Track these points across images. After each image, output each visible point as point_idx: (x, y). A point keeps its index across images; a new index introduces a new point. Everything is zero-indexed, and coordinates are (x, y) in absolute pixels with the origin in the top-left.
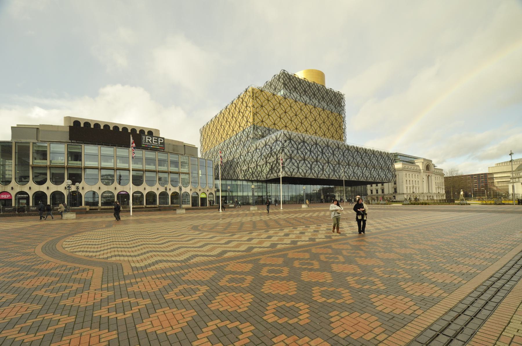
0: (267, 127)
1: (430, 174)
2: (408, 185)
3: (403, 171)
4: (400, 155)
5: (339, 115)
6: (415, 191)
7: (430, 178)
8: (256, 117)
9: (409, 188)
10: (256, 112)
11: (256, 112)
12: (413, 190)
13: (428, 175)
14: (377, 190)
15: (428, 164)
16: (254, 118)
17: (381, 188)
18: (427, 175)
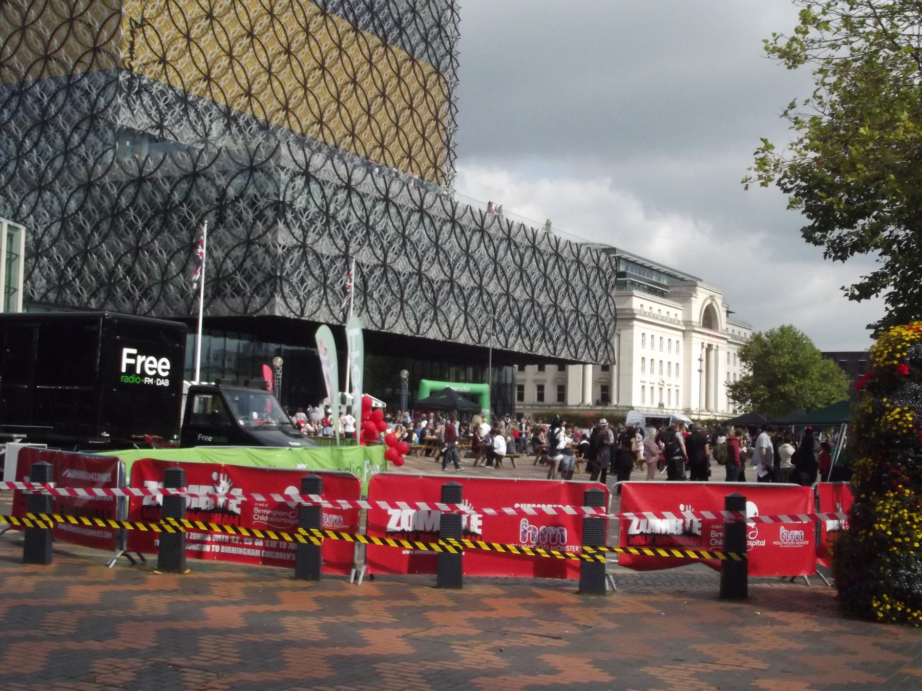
0: (179, 87)
1: (714, 342)
2: (648, 377)
3: (635, 323)
4: (626, 260)
5: (437, 71)
6: (665, 401)
7: (712, 353)
8: (139, 40)
9: (648, 389)
10: (143, 19)
11: (143, 19)
12: (661, 398)
13: (710, 346)
14: (541, 388)
15: (709, 302)
16: (132, 44)
17: (555, 381)
18: (706, 345)
